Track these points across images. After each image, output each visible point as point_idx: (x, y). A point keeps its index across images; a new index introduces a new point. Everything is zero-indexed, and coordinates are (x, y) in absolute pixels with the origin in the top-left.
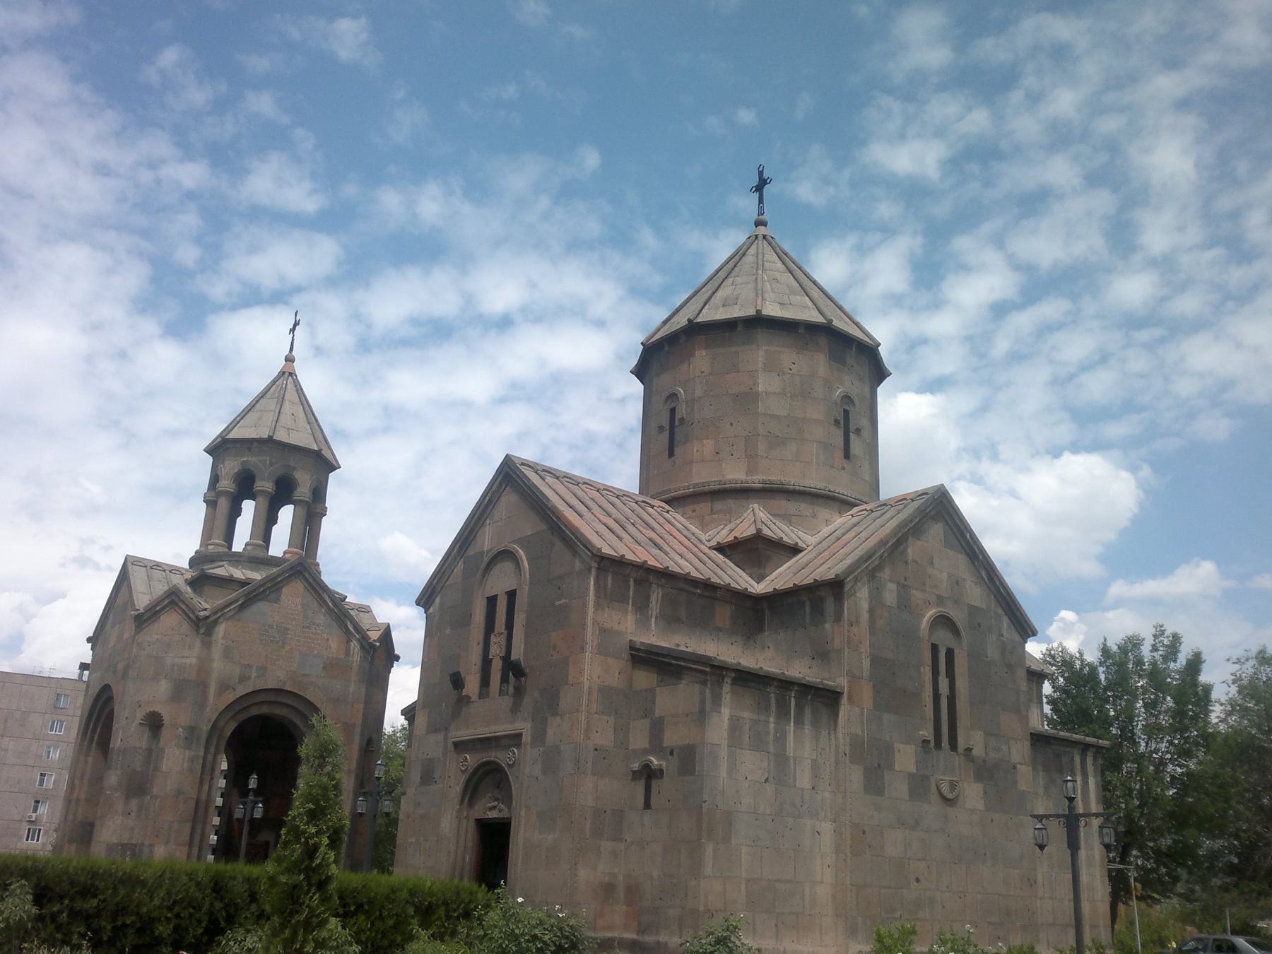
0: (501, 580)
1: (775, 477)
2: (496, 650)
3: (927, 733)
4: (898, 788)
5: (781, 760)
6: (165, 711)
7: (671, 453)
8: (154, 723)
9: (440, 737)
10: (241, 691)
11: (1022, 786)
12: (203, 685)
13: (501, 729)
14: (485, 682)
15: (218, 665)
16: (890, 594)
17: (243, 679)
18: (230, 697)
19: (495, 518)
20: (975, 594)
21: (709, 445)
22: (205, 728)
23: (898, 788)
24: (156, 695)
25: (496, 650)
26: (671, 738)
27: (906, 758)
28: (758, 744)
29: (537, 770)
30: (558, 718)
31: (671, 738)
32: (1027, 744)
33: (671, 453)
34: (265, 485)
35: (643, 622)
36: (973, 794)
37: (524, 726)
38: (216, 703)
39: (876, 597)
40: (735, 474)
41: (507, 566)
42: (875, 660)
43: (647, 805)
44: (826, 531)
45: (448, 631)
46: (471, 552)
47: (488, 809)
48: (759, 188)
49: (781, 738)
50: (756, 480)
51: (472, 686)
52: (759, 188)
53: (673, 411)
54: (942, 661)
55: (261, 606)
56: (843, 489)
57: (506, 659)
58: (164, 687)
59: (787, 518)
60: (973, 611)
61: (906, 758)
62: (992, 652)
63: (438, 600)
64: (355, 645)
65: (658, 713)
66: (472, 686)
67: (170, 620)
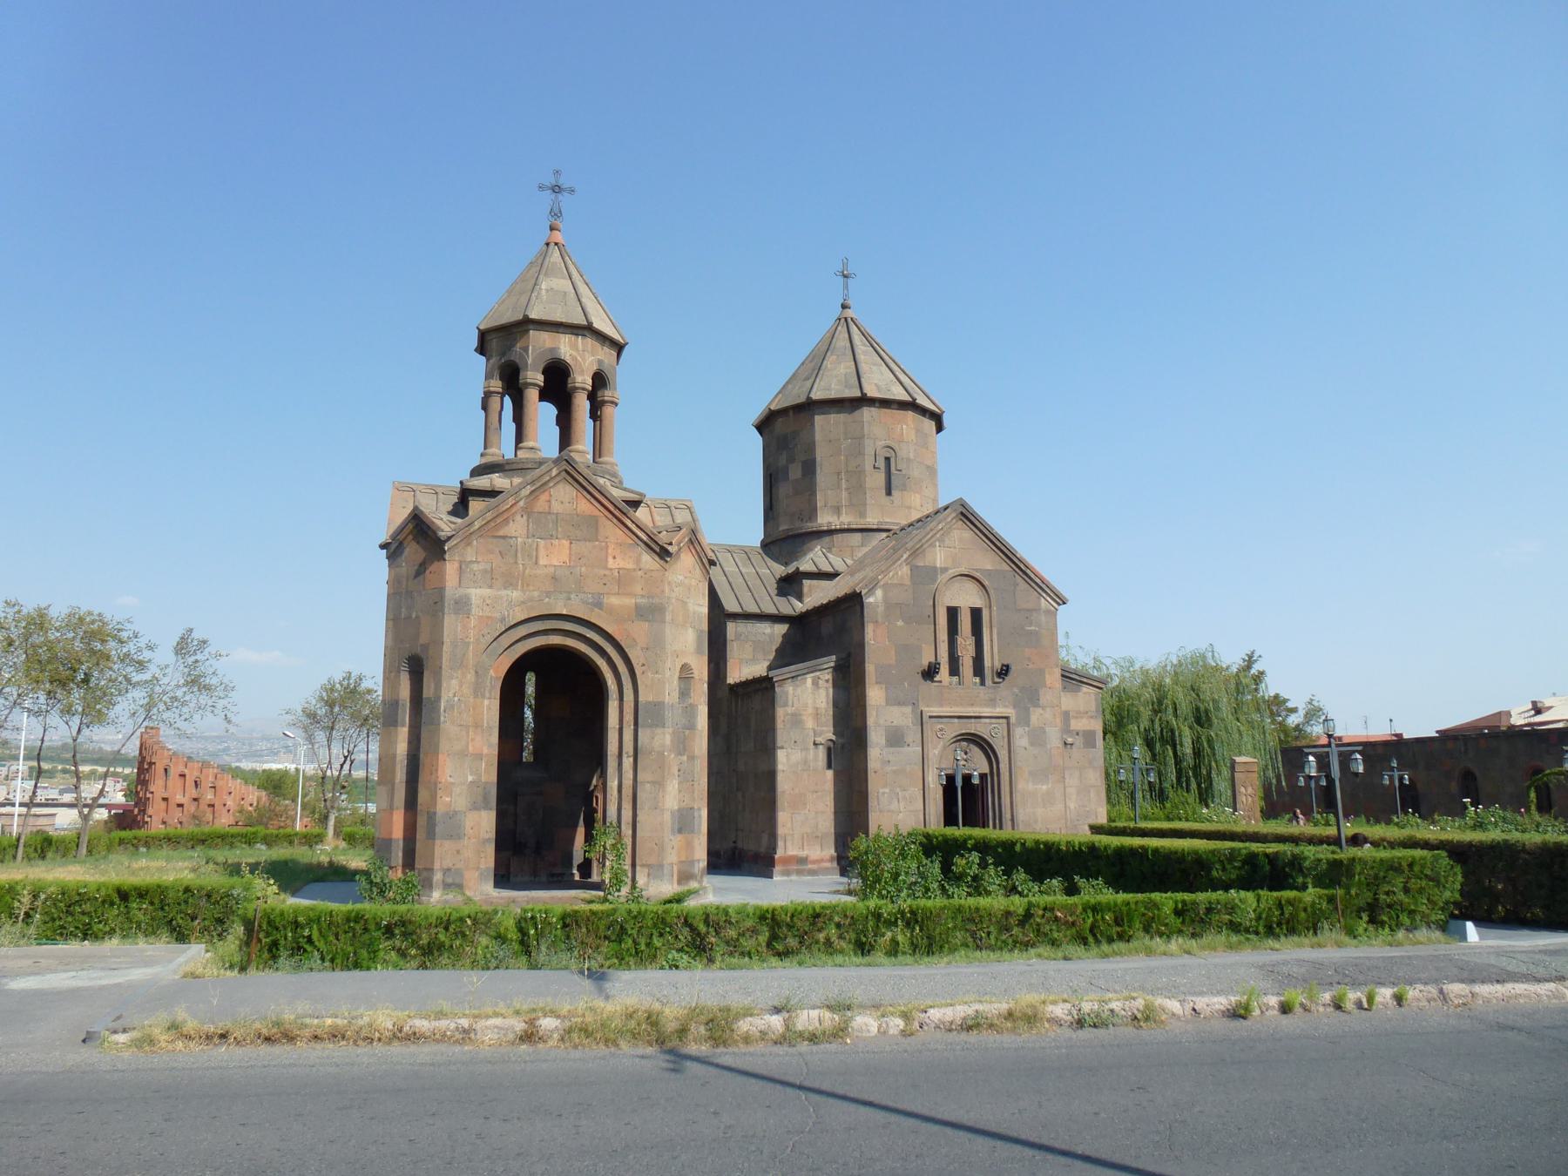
0: (966, 598)
7: (889, 493)
9: (908, 710)
13: (986, 711)
14: (954, 670)
19: (947, 542)
26: (1076, 725)
30: (1040, 710)
33: (889, 493)
37: (1009, 711)
41: (971, 586)
45: (900, 623)
53: (888, 459)
63: (879, 593)
65: (1064, 708)
66: (944, 674)
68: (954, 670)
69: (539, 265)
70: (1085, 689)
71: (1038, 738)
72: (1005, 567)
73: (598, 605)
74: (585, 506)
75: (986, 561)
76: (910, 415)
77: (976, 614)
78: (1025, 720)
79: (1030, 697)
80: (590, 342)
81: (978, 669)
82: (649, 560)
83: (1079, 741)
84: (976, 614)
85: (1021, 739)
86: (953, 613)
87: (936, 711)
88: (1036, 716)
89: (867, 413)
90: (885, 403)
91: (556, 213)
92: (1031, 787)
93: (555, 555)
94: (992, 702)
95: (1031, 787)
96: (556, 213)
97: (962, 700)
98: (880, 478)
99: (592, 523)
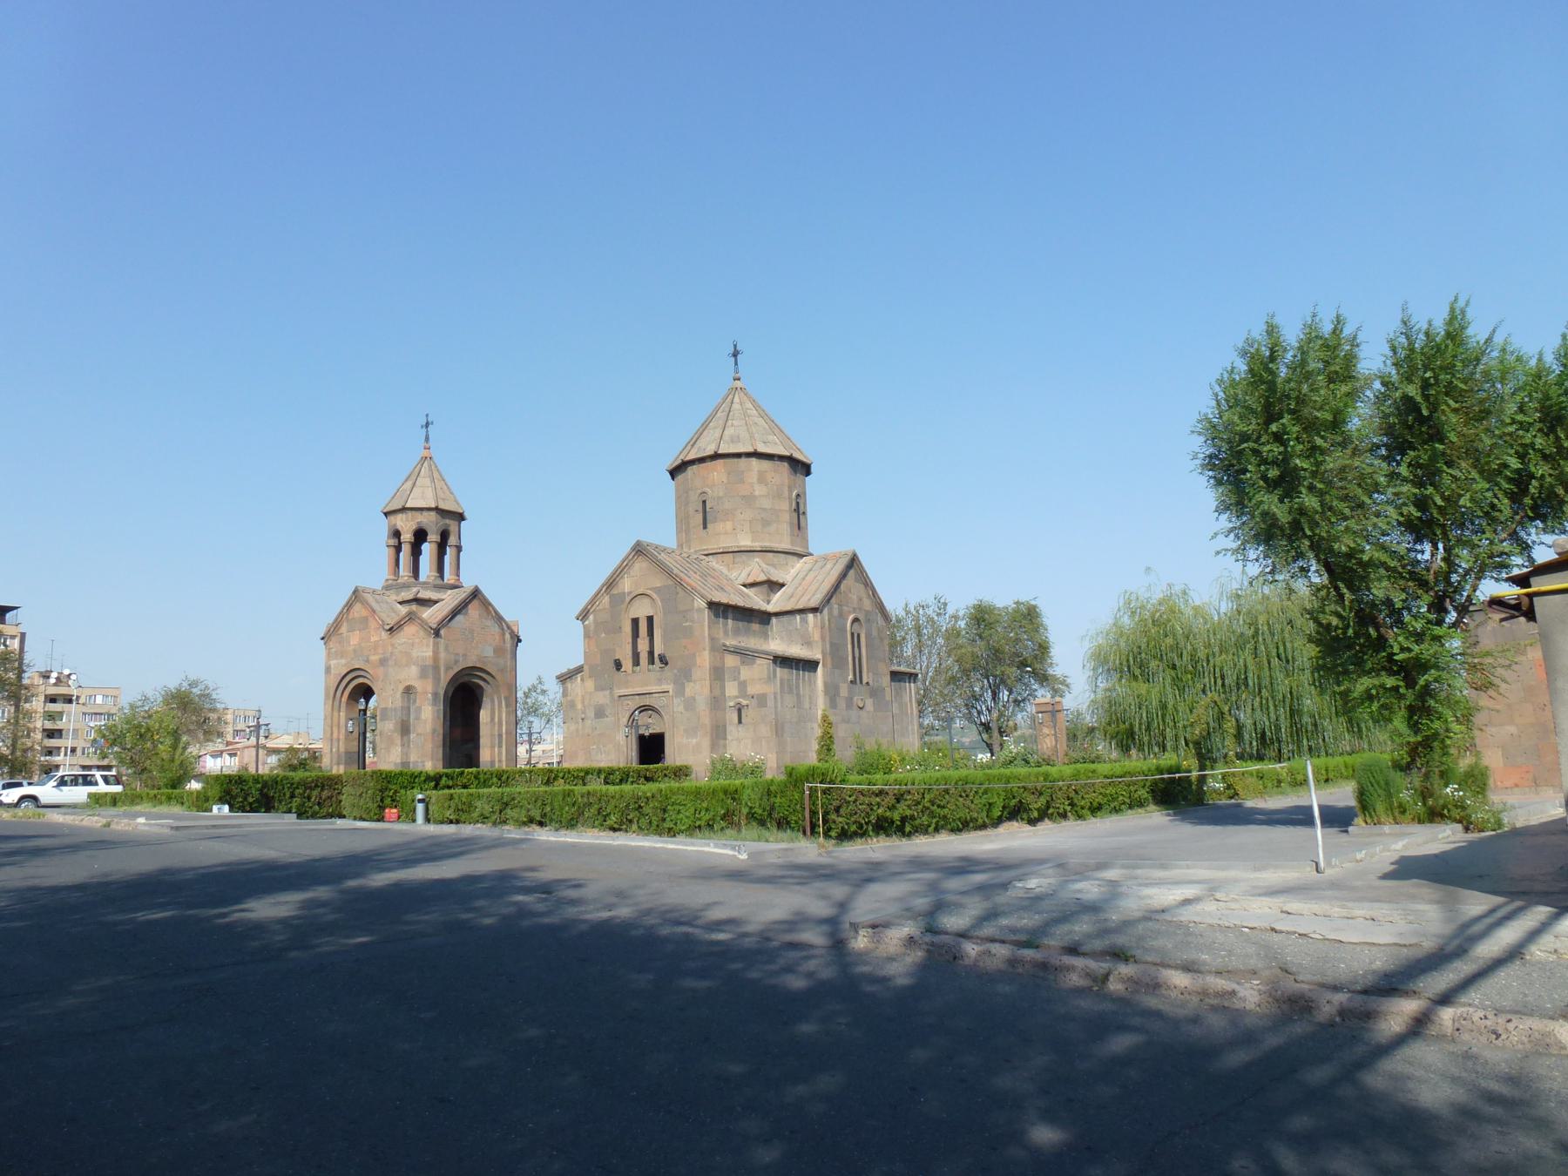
0: (641, 610)
1: (767, 544)
2: (643, 646)
3: (851, 677)
4: (842, 704)
5: (798, 695)
6: (418, 685)
7: (705, 527)
8: (408, 690)
10: (456, 669)
11: (888, 698)
12: (436, 668)
15: (442, 655)
16: (836, 612)
17: (456, 662)
18: (452, 673)
20: (867, 604)
21: (729, 525)
22: (442, 693)
23: (842, 704)
24: (411, 675)
25: (643, 646)
26: (751, 690)
27: (844, 690)
28: (790, 692)
29: (681, 708)
31: (751, 690)
32: (888, 677)
33: (705, 527)
34: (433, 537)
35: (726, 633)
36: (869, 703)
37: (670, 687)
38: (445, 678)
39: (830, 613)
40: (746, 542)
41: (646, 601)
42: (832, 644)
43: (740, 722)
44: (793, 572)
46: (615, 591)
47: (651, 726)
48: (735, 355)
49: (798, 687)
50: (757, 545)
51: (627, 664)
52: (735, 355)
54: (856, 639)
55: (459, 618)
56: (799, 549)
57: (651, 653)
58: (414, 670)
59: (774, 566)
60: (867, 612)
61: (844, 690)
62: (875, 633)
64: (508, 636)
66: (627, 664)
67: (410, 630)
68: (636, 662)
69: (413, 477)
70: (759, 661)
71: (690, 704)
72: (670, 582)
73: (368, 661)
74: (364, 613)
75: (658, 581)
76: (720, 462)
77: (650, 619)
78: (680, 691)
79: (685, 675)
80: (410, 514)
81: (651, 661)
82: (384, 635)
83: (754, 702)
84: (650, 619)
85: (678, 706)
86: (635, 622)
87: (623, 692)
88: (689, 689)
89: (691, 470)
90: (702, 460)
91: (427, 439)
92: (685, 741)
93: (355, 639)
94: (660, 681)
95: (685, 741)
96: (427, 439)
97: (646, 681)
98: (700, 516)
99: (366, 619)
